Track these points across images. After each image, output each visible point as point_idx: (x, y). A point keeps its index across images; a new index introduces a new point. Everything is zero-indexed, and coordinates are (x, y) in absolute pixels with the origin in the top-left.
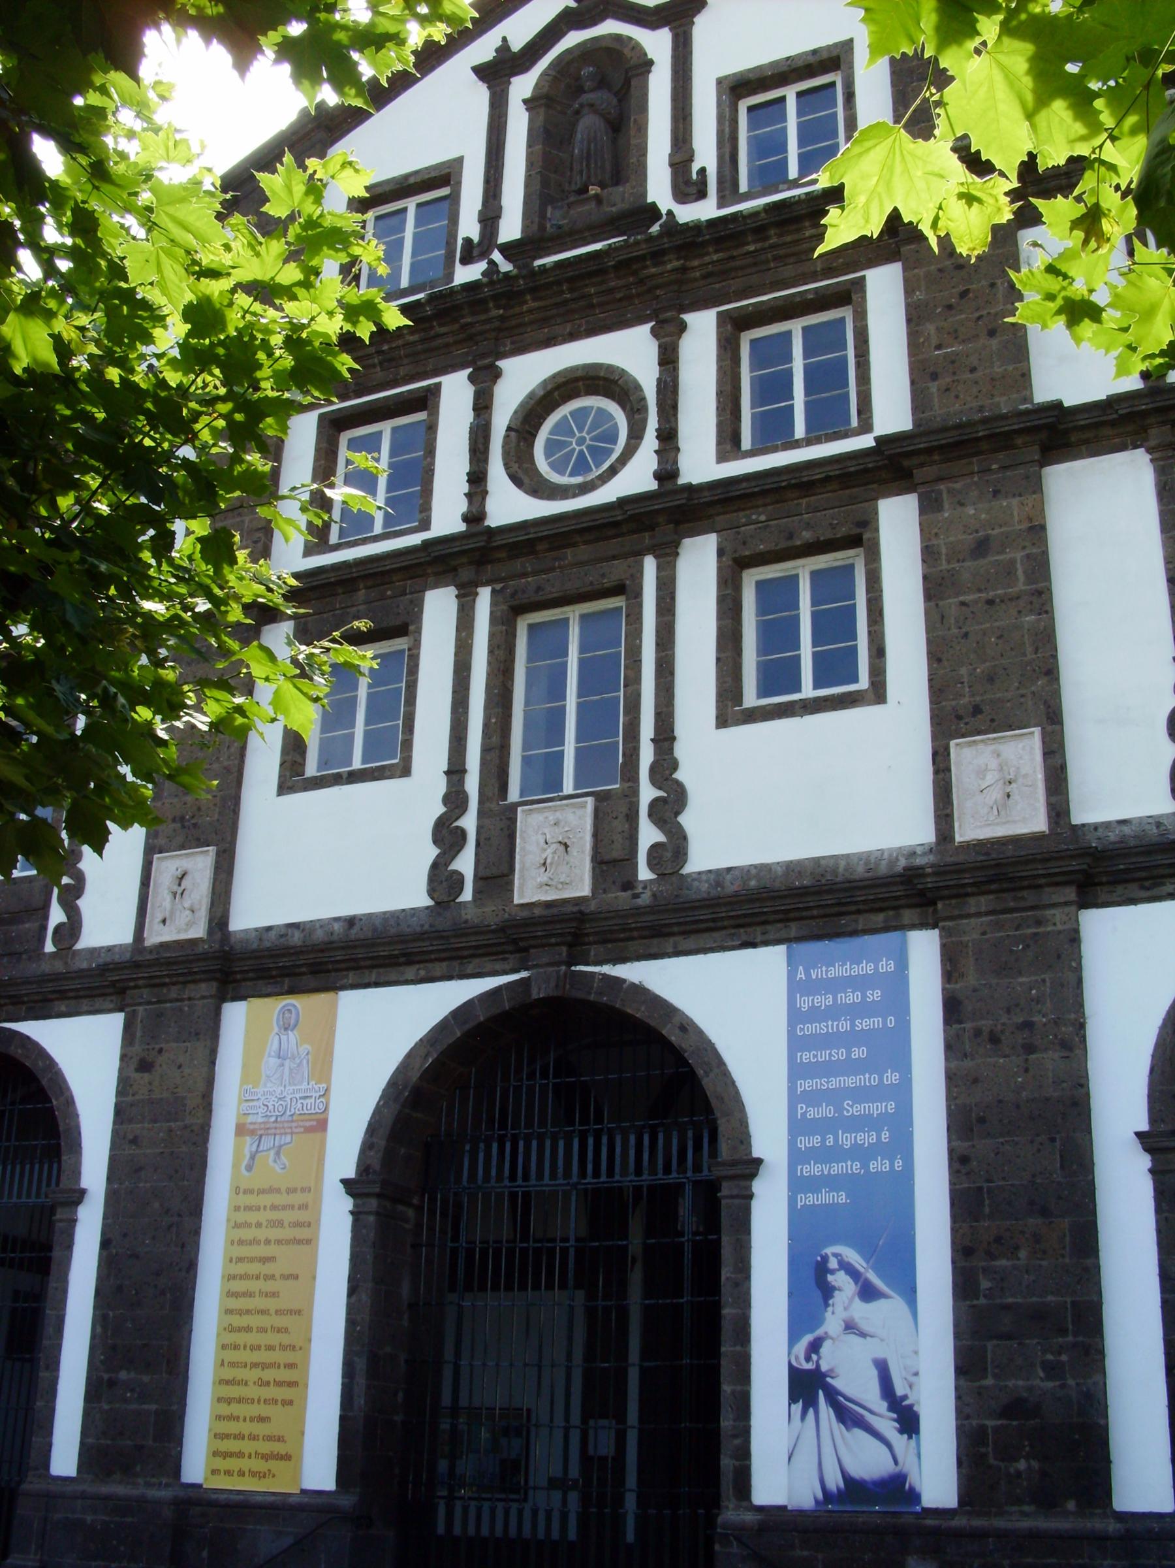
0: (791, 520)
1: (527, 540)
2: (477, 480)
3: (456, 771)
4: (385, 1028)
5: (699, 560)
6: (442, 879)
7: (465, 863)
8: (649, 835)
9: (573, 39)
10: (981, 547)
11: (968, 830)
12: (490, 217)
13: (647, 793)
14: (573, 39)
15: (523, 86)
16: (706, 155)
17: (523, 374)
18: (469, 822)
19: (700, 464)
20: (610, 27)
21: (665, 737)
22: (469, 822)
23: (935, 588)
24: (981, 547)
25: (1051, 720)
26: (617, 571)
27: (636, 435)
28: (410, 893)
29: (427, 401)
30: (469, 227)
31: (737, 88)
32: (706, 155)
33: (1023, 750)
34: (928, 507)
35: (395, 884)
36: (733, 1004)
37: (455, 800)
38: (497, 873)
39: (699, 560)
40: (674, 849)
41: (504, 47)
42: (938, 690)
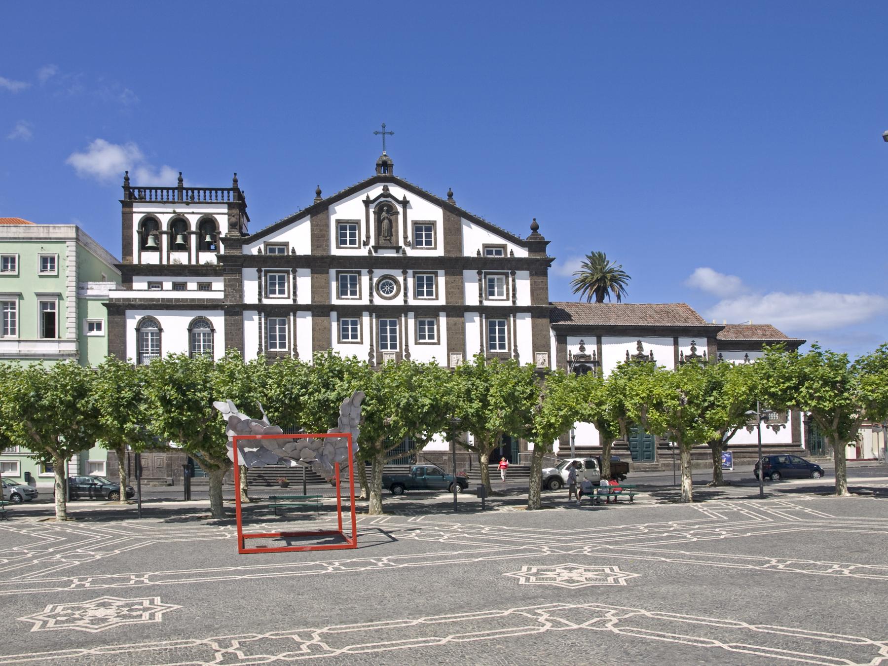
2: (371, 294)
3: (372, 345)
7: (374, 360)
9: (382, 199)
10: (455, 324)
12: (368, 237)
13: (404, 353)
14: (382, 199)
16: (410, 239)
17: (378, 273)
18: (375, 354)
19: (412, 302)
20: (389, 199)
21: (407, 346)
22: (375, 354)
23: (448, 329)
30: (363, 238)
31: (415, 223)
32: (410, 239)
41: (368, 197)
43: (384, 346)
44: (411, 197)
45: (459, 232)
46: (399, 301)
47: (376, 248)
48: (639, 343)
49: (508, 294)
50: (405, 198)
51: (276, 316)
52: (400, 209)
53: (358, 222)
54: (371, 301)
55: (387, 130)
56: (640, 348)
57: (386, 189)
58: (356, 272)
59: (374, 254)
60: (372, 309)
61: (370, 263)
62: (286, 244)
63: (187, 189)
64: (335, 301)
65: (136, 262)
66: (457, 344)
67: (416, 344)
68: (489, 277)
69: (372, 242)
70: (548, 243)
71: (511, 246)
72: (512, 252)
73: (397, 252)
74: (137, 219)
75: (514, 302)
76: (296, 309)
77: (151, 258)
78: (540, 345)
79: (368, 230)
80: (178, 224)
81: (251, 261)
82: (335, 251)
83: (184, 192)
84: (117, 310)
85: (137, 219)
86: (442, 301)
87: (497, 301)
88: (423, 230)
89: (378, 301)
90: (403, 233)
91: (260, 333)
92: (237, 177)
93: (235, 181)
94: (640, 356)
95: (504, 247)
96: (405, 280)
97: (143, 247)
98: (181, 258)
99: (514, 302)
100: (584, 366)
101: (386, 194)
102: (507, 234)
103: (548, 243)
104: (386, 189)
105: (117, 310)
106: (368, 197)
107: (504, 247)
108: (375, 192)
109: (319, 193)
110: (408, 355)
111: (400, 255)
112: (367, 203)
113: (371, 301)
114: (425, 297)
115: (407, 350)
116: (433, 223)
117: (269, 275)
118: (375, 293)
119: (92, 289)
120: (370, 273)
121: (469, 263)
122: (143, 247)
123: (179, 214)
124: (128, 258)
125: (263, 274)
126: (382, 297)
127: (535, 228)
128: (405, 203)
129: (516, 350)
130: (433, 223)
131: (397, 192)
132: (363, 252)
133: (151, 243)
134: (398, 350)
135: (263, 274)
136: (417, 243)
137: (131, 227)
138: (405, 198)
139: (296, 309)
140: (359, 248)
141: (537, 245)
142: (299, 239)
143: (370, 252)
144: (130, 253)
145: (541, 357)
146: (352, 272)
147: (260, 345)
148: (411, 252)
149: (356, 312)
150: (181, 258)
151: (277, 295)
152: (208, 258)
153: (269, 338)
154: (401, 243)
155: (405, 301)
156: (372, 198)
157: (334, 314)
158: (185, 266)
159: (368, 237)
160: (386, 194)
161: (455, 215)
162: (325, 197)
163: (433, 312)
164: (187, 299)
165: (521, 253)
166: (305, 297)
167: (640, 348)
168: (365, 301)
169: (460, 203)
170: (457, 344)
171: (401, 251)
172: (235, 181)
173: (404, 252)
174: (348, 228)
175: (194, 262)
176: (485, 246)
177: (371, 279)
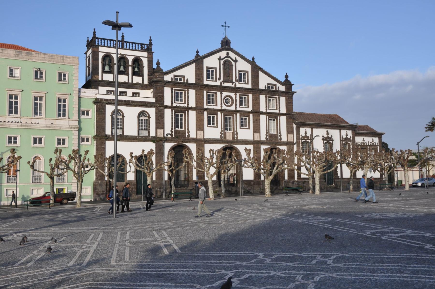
0: (245, 114)
1: (225, 110)
3: (222, 128)
4: (218, 147)
5: (238, 115)
6: (221, 136)
7: (223, 136)
8: (235, 136)
9: (226, 59)
10: (257, 120)
11: (255, 140)
12: (220, 76)
14: (226, 59)
15: (222, 62)
16: (237, 78)
17: (225, 94)
20: (229, 59)
23: (254, 122)
24: (257, 120)
25: (260, 133)
26: (233, 114)
27: (232, 103)
28: (219, 137)
29: (216, 93)
30: (218, 77)
31: (240, 71)
32: (237, 78)
33: (259, 134)
34: (253, 116)
35: (218, 137)
36: (241, 148)
37: (222, 130)
38: (225, 137)
39: (238, 115)
40: (237, 137)
41: (220, 57)
42: (254, 129)
43: (226, 129)
44: (238, 58)
45: (258, 76)
46: (233, 108)
47: (224, 81)
48: (327, 132)
49: (277, 107)
50: (236, 59)
51: (180, 112)
52: (233, 63)
53: (216, 69)
54: (221, 107)
55: (224, 25)
56: (328, 134)
57: (228, 54)
58: (215, 93)
59: (223, 85)
60: (221, 111)
61: (222, 89)
62: (184, 77)
63: (126, 42)
64: (206, 106)
65: (100, 79)
66: (257, 130)
67: (208, 127)
68: (269, 98)
69: (222, 79)
70: (293, 85)
71: (278, 85)
72: (278, 88)
73: (233, 84)
74: (101, 55)
75: (279, 111)
76: (189, 109)
77: (108, 77)
78: (290, 131)
79: (220, 73)
80: (123, 59)
81: (168, 83)
82: (206, 82)
83: (125, 43)
84: (100, 104)
85: (101, 55)
86: (250, 109)
87: (273, 110)
88: (242, 75)
89: (224, 107)
90: (235, 76)
91: (172, 120)
92: (151, 38)
93: (150, 40)
94: (328, 137)
95: (275, 85)
96: (236, 97)
97: (104, 72)
98: (123, 78)
99: (279, 111)
100: (307, 142)
101: (228, 56)
102: (277, 79)
103: (293, 85)
104: (228, 54)
105: (100, 104)
106: (220, 57)
107: (275, 85)
108: (223, 54)
109: (197, 52)
110: (237, 134)
111: (234, 86)
112: (220, 59)
113: (221, 107)
114: (243, 106)
115: (236, 131)
116: (247, 72)
117: (183, 92)
118: (223, 104)
119: (85, 92)
120: (221, 93)
121: (262, 92)
122: (104, 72)
123: (123, 55)
124: (96, 76)
125: (173, 91)
126: (226, 105)
127: (287, 77)
128: (236, 61)
129: (280, 133)
130: (247, 72)
131: (231, 54)
132: (218, 83)
133: (107, 68)
134: (232, 131)
135: (173, 91)
136: (240, 81)
137: (98, 59)
138: (236, 59)
139: (189, 109)
140: (216, 81)
141: (288, 84)
142: (189, 74)
143: (221, 83)
144: (97, 74)
145: (290, 136)
146: (213, 93)
147: (172, 126)
148: (239, 85)
149: (215, 112)
150: (123, 78)
151: (179, 102)
152: (137, 80)
153: (176, 123)
154: (234, 80)
155: (236, 108)
156: (222, 58)
157: (205, 113)
158: (140, 84)
159: (220, 76)
160: (228, 56)
161: (256, 69)
162: (201, 54)
163: (246, 114)
164: (137, 101)
165: (282, 88)
166: (192, 103)
167: (328, 134)
168: (219, 107)
169: (258, 63)
170: (257, 130)
171: (234, 84)
172: (150, 40)
173: (235, 85)
174: (211, 72)
175: (130, 81)
176: (268, 84)
177: (221, 96)
